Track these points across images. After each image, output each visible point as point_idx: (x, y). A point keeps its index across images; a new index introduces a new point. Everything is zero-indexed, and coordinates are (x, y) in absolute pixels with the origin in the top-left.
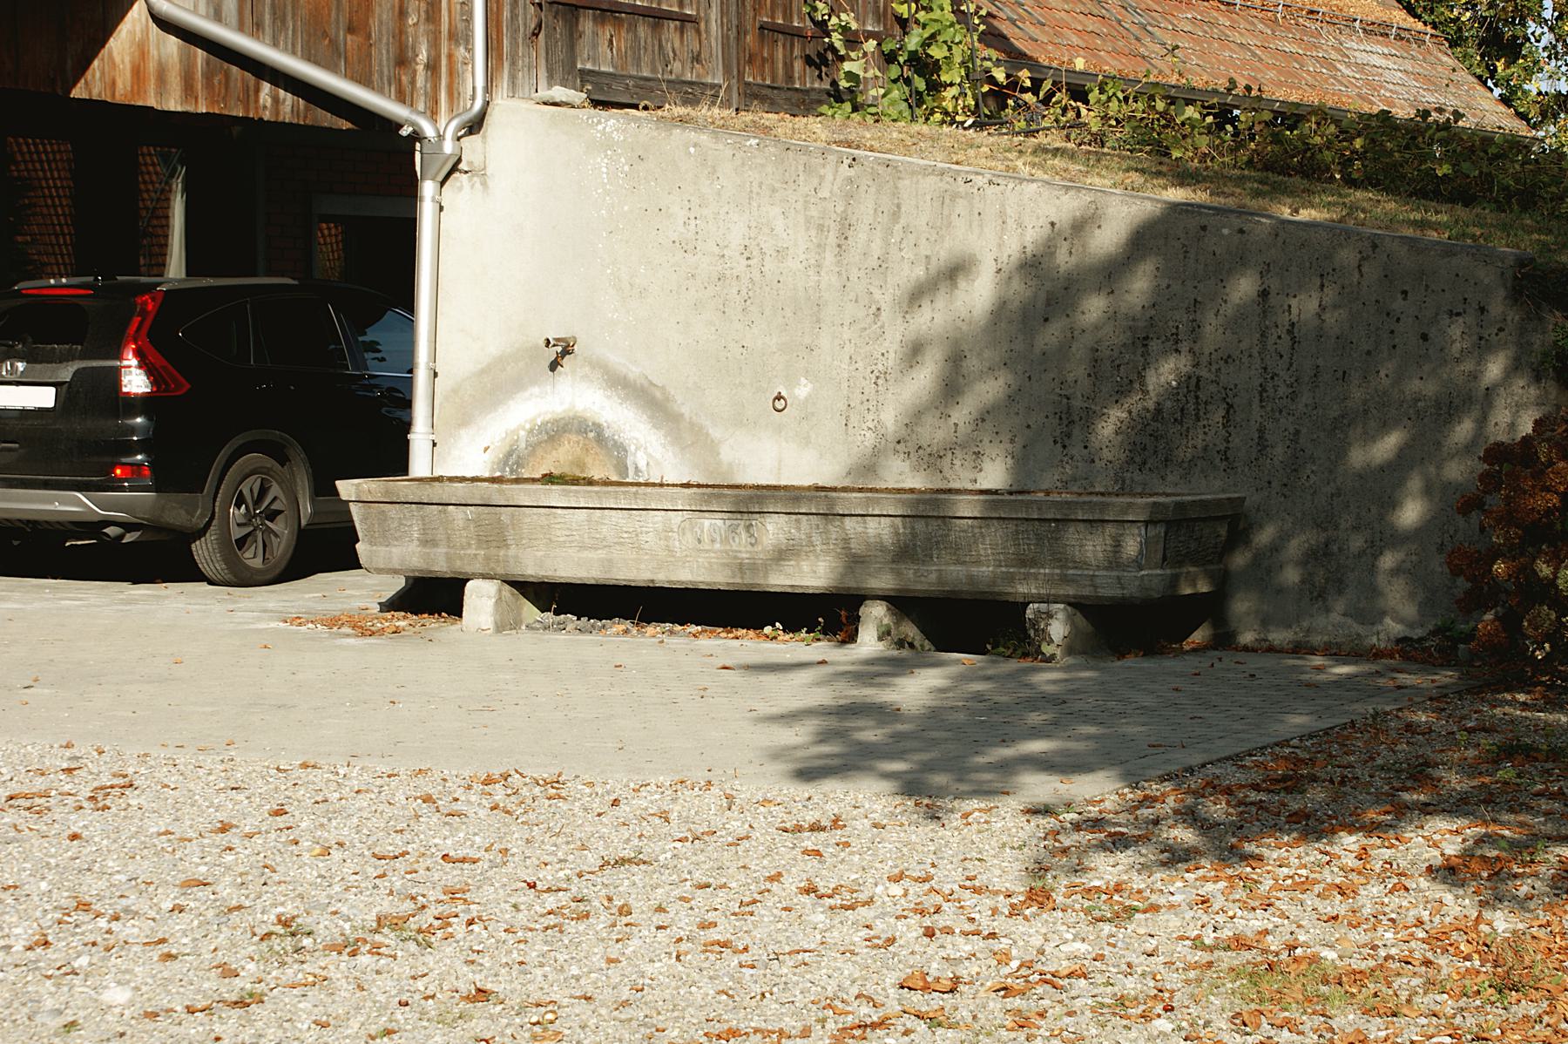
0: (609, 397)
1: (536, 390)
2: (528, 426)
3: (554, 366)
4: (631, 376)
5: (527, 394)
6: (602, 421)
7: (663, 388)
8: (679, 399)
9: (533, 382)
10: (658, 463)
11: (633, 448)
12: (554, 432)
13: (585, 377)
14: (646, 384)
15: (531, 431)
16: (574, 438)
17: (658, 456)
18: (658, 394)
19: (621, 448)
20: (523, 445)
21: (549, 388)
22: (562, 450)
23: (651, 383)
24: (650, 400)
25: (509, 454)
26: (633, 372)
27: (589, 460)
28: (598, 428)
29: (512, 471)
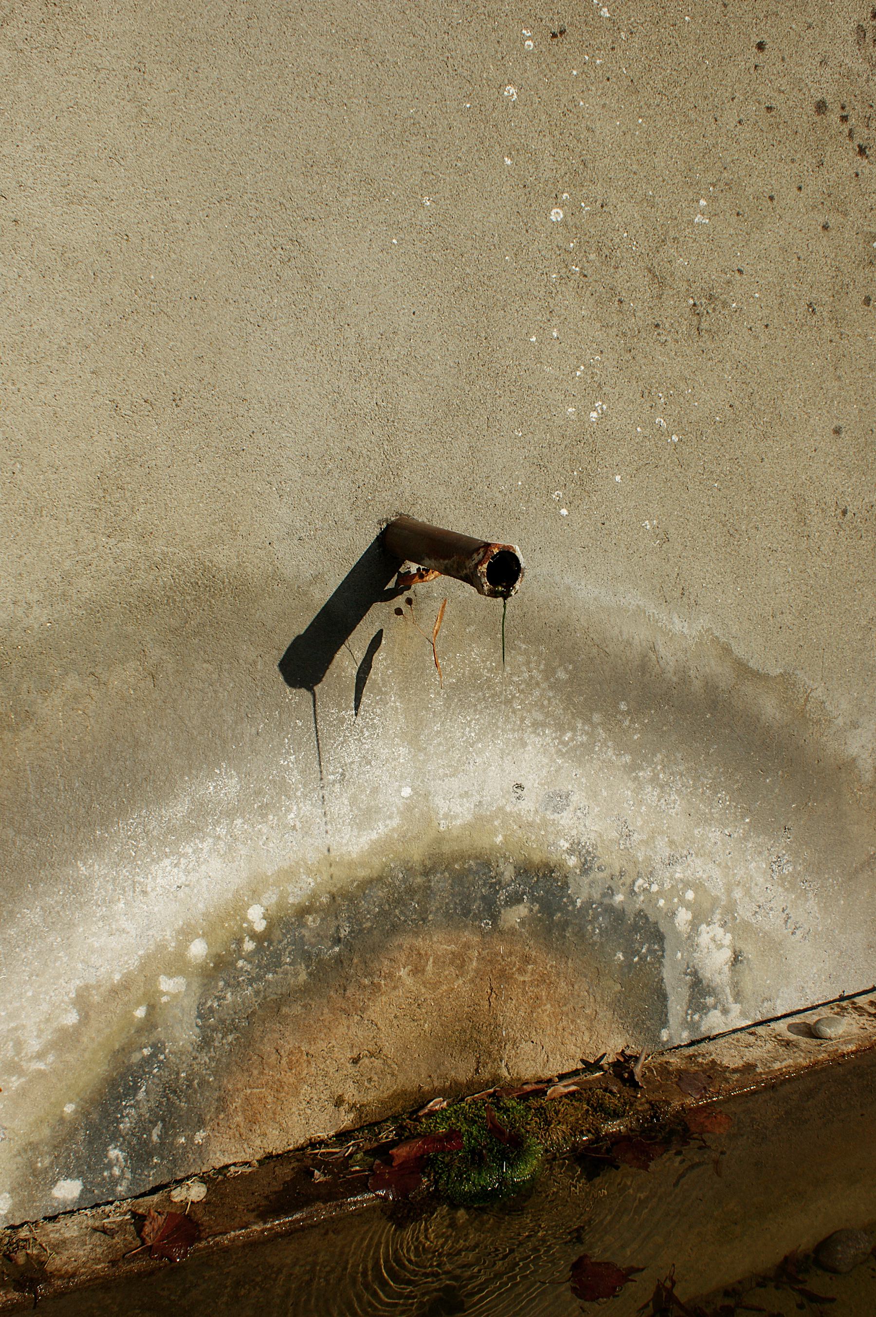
0: (580, 754)
1: (225, 785)
2: (198, 949)
3: (306, 662)
4: (668, 657)
5: (179, 809)
6: (560, 851)
7: (787, 680)
8: (841, 707)
9: (207, 748)
10: (773, 946)
11: (683, 916)
12: (342, 938)
13: (467, 692)
14: (720, 671)
15: (220, 967)
16: (439, 943)
17: (772, 922)
18: (770, 708)
19: (644, 933)
20: (183, 1035)
21: (292, 764)
22: (380, 1009)
23: (743, 670)
24: (729, 730)
25: (118, 1087)
26: (677, 635)
27: (511, 1011)
28: (543, 882)
29: (140, 1156)
